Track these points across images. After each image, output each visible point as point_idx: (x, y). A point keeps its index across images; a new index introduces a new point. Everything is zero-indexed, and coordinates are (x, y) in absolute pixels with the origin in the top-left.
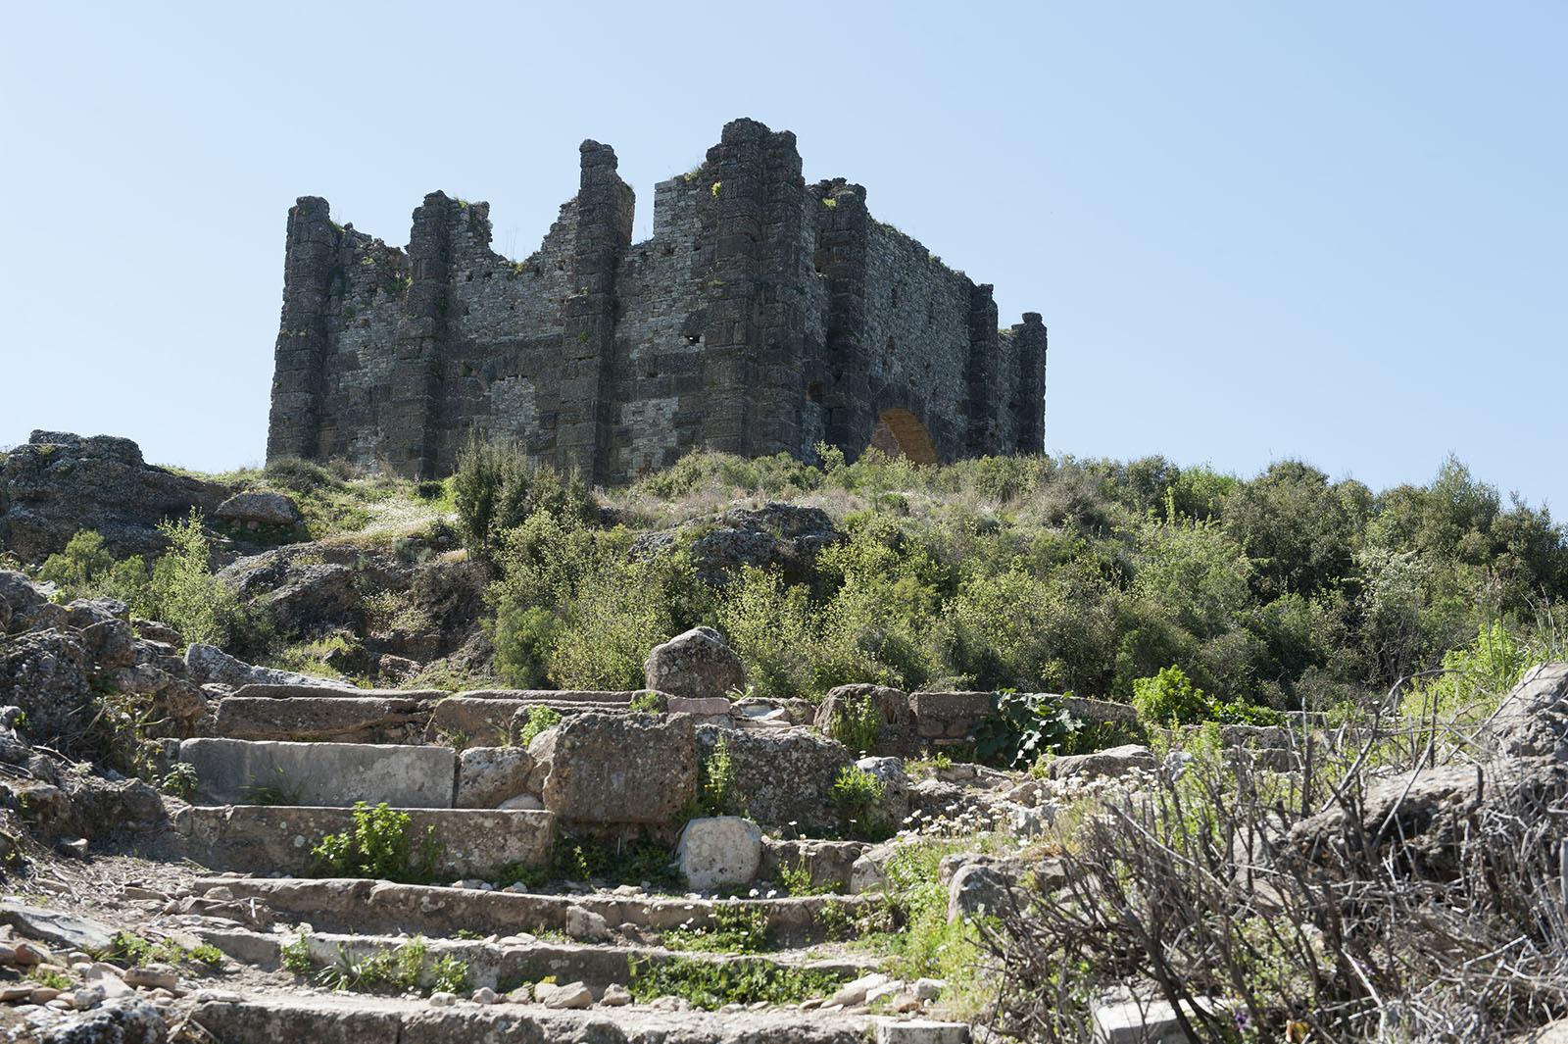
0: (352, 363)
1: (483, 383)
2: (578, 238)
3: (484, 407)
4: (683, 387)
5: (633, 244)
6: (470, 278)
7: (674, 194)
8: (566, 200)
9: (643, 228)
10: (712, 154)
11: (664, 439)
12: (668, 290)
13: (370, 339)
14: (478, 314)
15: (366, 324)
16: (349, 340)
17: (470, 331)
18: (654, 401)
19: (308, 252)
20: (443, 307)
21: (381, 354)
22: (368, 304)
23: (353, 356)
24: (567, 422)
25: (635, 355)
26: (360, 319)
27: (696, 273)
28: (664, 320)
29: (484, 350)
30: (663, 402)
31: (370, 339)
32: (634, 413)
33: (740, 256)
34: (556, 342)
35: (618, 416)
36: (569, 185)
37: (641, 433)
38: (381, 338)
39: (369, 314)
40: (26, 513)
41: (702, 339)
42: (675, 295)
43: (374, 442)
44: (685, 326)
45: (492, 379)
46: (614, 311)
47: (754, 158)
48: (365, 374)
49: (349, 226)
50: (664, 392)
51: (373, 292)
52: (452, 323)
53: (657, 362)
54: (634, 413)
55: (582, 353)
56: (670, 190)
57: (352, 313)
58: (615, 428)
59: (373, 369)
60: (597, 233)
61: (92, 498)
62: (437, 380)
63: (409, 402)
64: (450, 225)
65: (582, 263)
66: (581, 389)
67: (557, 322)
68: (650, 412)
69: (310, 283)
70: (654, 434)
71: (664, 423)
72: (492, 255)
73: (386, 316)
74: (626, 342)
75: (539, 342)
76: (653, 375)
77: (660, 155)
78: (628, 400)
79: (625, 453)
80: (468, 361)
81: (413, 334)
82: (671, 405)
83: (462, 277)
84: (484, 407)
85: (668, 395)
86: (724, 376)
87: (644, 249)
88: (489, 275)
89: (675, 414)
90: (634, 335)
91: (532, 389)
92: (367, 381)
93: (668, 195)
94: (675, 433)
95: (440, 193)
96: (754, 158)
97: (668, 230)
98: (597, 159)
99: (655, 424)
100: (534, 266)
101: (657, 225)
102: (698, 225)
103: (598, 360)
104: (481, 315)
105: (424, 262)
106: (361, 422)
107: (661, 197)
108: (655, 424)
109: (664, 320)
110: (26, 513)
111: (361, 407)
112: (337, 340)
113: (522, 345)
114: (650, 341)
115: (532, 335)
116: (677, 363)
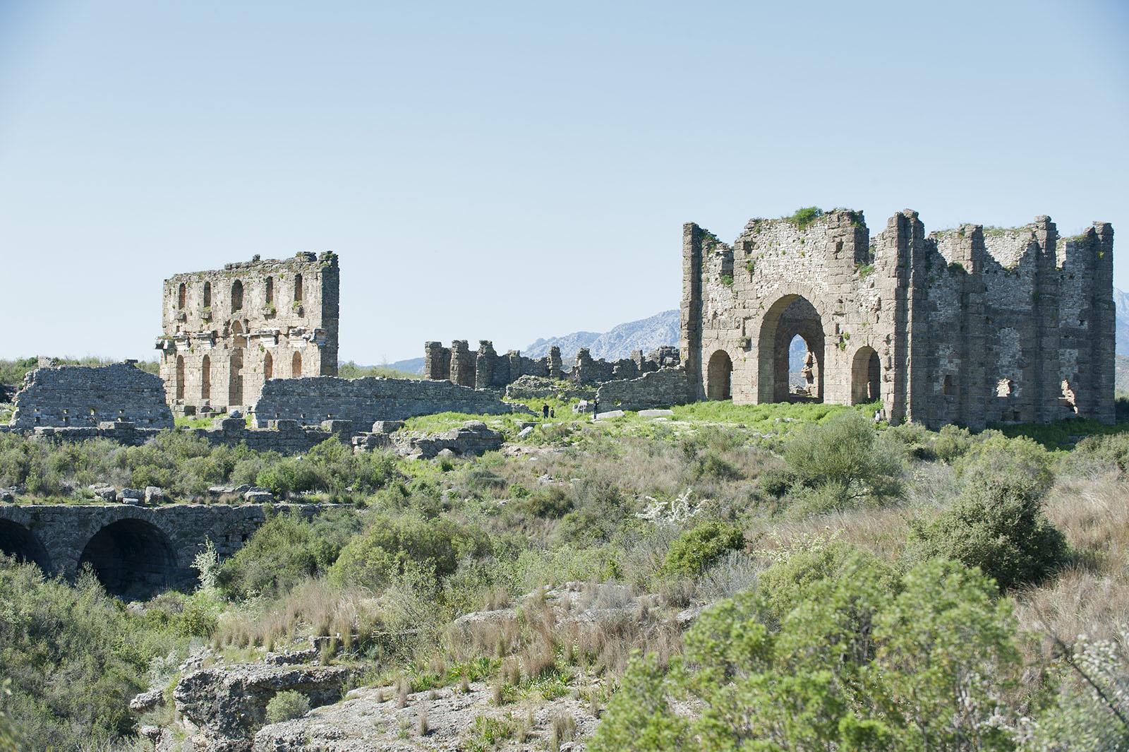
1: (997, 329)
4: (1078, 345)
11: (1073, 369)
17: (989, 300)
18: (1068, 350)
21: (948, 305)
27: (1083, 291)
29: (996, 312)
38: (947, 296)
48: (941, 315)
57: (932, 280)
63: (979, 338)
67: (1027, 303)
68: (1067, 355)
70: (1069, 366)
75: (1020, 312)
81: (978, 301)
82: (1076, 353)
85: (1073, 348)
92: (942, 319)
93: (1071, 249)
98: (1050, 227)
99: (1069, 361)
100: (1015, 272)
104: (994, 292)
106: (942, 341)
113: (1012, 312)
114: (1066, 320)
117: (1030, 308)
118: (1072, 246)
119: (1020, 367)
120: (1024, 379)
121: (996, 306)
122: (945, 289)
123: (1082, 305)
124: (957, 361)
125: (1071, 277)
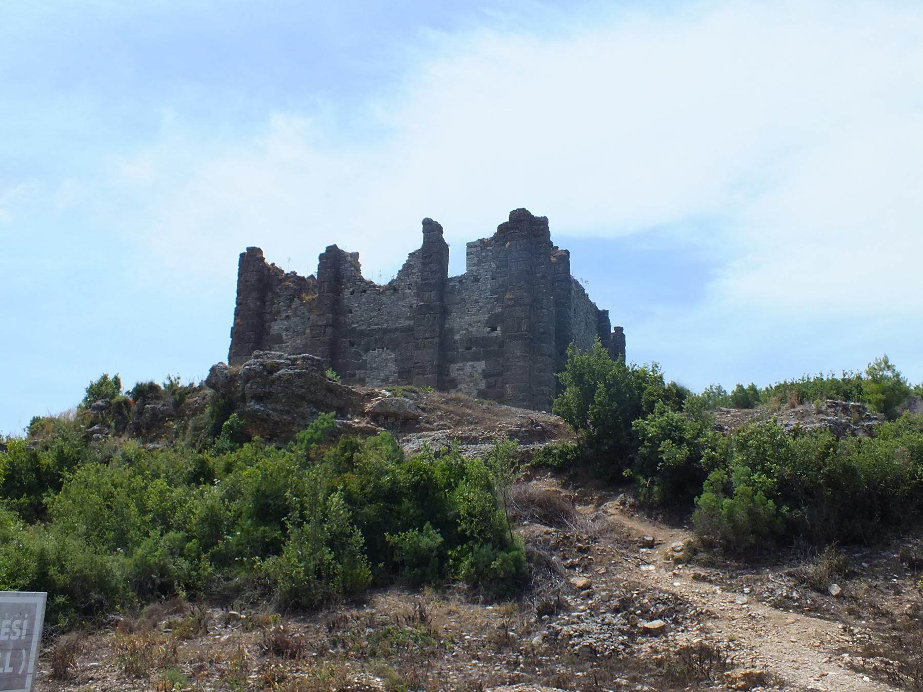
2: (422, 272)
3: (363, 366)
4: (487, 356)
5: (451, 274)
6: (352, 293)
7: (477, 249)
8: (412, 251)
9: (457, 266)
10: (502, 228)
11: (477, 384)
12: (477, 302)
13: (290, 327)
14: (359, 313)
15: (288, 317)
17: (353, 323)
18: (470, 363)
19: (253, 278)
20: (337, 308)
21: (297, 335)
22: (289, 306)
23: (280, 336)
24: (419, 374)
25: (457, 337)
26: (284, 315)
27: (493, 293)
28: (476, 318)
29: (362, 334)
30: (476, 364)
31: (290, 327)
32: (458, 370)
33: (522, 283)
34: (410, 329)
35: (448, 372)
36: (416, 242)
39: (289, 313)
40: (257, 407)
41: (499, 329)
42: (481, 304)
44: (488, 321)
45: (367, 350)
46: (445, 313)
47: (525, 229)
49: (273, 264)
50: (475, 357)
51: (292, 300)
52: (342, 318)
53: (471, 342)
54: (458, 370)
55: (427, 335)
56: (476, 246)
57: (278, 312)
58: (446, 378)
60: (434, 269)
61: (302, 398)
64: (337, 264)
66: (428, 356)
67: (408, 318)
69: (254, 295)
71: (476, 375)
72: (362, 280)
73: (300, 314)
74: (452, 331)
75: (397, 329)
76: (469, 349)
77: (470, 225)
78: (454, 362)
80: (352, 340)
81: (320, 323)
82: (481, 365)
83: (347, 293)
85: (479, 360)
86: (516, 349)
87: (460, 279)
88: (365, 291)
89: (483, 370)
90: (457, 326)
91: (393, 356)
93: (475, 249)
94: (484, 381)
95: (335, 246)
96: (525, 229)
97: (475, 268)
98: (432, 229)
99: (471, 376)
100: (393, 287)
101: (468, 265)
102: (494, 266)
103: (436, 340)
104: (359, 315)
105: (326, 284)
107: (470, 250)
108: (471, 376)
110: (257, 407)
112: (270, 327)
113: (386, 331)
114: (466, 329)
116: (483, 342)
118: (476, 246)
121: (363, 327)
122: (293, 319)
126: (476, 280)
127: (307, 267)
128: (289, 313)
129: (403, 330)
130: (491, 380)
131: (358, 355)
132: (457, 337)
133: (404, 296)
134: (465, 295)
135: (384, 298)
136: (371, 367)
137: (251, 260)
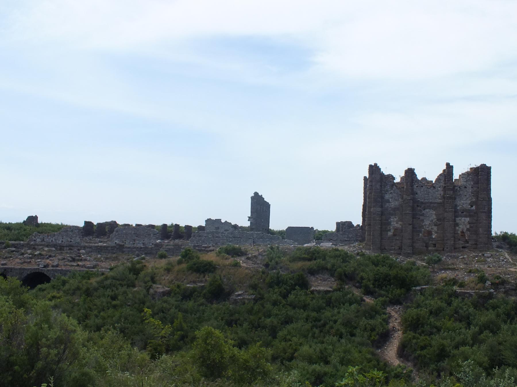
0: (388, 201)
3: (423, 215)
4: (470, 216)
12: (466, 196)
16: (387, 197)
22: (392, 189)
25: (458, 208)
27: (472, 193)
28: (466, 202)
29: (422, 203)
30: (466, 218)
37: (461, 224)
39: (392, 191)
43: (395, 219)
46: (455, 199)
50: (466, 216)
57: (387, 191)
59: (394, 204)
62: (413, 209)
65: (445, 189)
67: (440, 199)
68: (463, 220)
69: (379, 184)
71: (466, 223)
75: (435, 203)
78: (457, 217)
79: (457, 228)
82: (468, 219)
83: (415, 186)
84: (423, 215)
104: (421, 195)
106: (392, 215)
108: (464, 223)
109: (466, 202)
111: (392, 212)
113: (431, 203)
115: (433, 201)
116: (469, 211)
117: (441, 201)
119: (435, 225)
120: (438, 230)
121: (422, 201)
123: (471, 199)
124: (400, 223)
125: (465, 187)
126: (465, 187)
127: (398, 175)
128: (392, 191)
129: (438, 203)
130: (472, 225)
131: (421, 211)
132: (458, 208)
133: (438, 191)
134: (461, 192)
135: (430, 191)
136: (426, 216)
137: (374, 169)
